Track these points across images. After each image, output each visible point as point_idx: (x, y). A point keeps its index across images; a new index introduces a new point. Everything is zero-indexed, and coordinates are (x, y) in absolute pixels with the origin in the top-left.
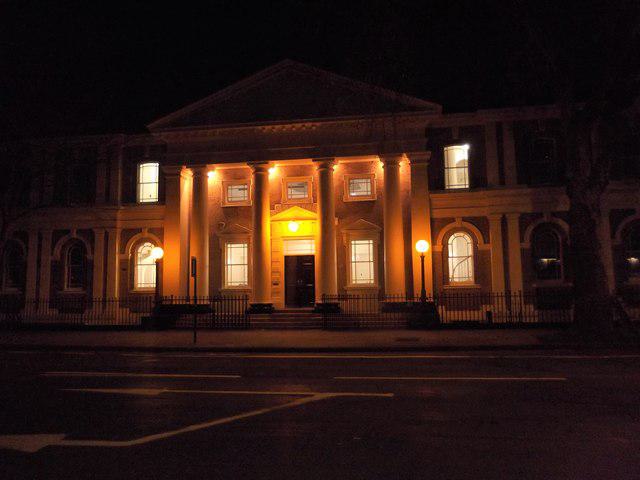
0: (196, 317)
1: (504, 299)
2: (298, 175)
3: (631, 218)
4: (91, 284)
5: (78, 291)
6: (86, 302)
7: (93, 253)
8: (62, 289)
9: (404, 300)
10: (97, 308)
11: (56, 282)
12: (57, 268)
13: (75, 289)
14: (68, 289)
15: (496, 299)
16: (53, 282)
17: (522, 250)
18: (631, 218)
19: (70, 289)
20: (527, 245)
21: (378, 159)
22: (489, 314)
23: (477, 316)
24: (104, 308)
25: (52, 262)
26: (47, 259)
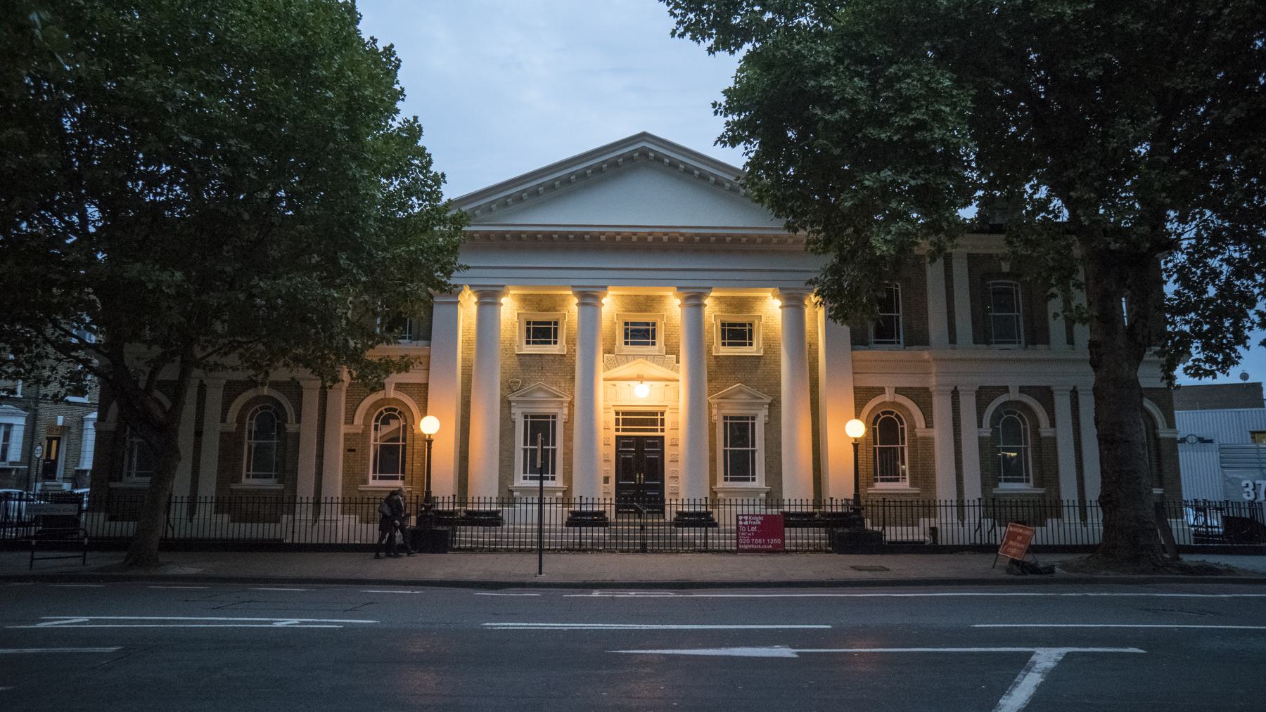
0: (706, 532)
1: (955, 509)
2: (641, 311)
3: (1003, 398)
4: (295, 471)
5: (271, 484)
6: (285, 502)
7: (298, 421)
8: (365, 481)
9: (811, 510)
10: (304, 514)
11: (228, 471)
12: (230, 444)
13: (256, 481)
14: (248, 482)
15: (1065, 509)
16: (221, 471)
17: (981, 439)
18: (1003, 398)
19: (252, 481)
20: (987, 432)
21: (769, 294)
22: (934, 531)
23: (916, 533)
24: (317, 513)
25: (221, 433)
26: (339, 431)
